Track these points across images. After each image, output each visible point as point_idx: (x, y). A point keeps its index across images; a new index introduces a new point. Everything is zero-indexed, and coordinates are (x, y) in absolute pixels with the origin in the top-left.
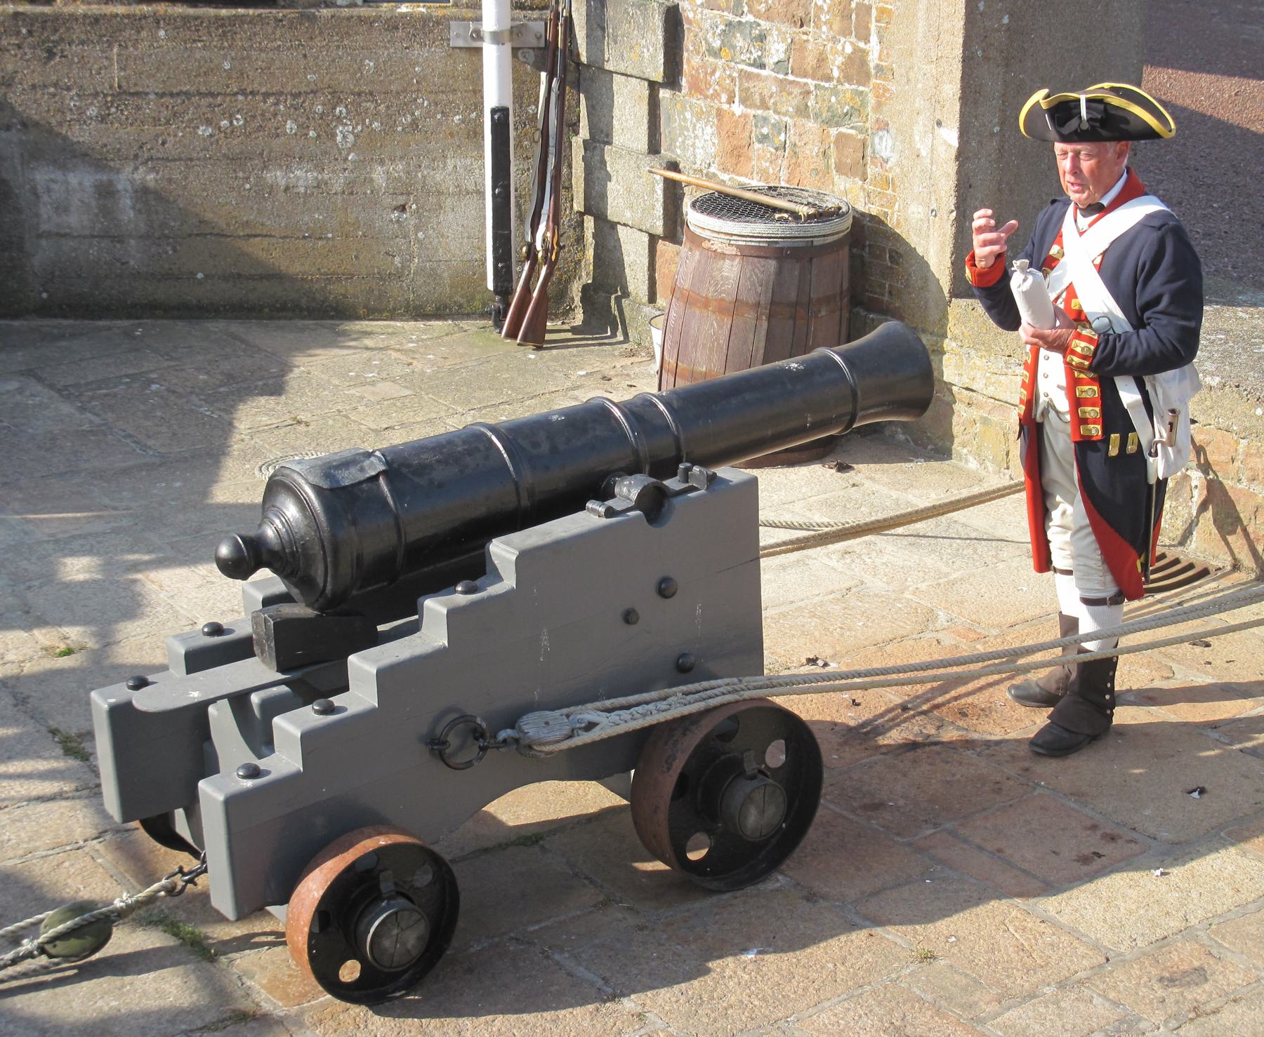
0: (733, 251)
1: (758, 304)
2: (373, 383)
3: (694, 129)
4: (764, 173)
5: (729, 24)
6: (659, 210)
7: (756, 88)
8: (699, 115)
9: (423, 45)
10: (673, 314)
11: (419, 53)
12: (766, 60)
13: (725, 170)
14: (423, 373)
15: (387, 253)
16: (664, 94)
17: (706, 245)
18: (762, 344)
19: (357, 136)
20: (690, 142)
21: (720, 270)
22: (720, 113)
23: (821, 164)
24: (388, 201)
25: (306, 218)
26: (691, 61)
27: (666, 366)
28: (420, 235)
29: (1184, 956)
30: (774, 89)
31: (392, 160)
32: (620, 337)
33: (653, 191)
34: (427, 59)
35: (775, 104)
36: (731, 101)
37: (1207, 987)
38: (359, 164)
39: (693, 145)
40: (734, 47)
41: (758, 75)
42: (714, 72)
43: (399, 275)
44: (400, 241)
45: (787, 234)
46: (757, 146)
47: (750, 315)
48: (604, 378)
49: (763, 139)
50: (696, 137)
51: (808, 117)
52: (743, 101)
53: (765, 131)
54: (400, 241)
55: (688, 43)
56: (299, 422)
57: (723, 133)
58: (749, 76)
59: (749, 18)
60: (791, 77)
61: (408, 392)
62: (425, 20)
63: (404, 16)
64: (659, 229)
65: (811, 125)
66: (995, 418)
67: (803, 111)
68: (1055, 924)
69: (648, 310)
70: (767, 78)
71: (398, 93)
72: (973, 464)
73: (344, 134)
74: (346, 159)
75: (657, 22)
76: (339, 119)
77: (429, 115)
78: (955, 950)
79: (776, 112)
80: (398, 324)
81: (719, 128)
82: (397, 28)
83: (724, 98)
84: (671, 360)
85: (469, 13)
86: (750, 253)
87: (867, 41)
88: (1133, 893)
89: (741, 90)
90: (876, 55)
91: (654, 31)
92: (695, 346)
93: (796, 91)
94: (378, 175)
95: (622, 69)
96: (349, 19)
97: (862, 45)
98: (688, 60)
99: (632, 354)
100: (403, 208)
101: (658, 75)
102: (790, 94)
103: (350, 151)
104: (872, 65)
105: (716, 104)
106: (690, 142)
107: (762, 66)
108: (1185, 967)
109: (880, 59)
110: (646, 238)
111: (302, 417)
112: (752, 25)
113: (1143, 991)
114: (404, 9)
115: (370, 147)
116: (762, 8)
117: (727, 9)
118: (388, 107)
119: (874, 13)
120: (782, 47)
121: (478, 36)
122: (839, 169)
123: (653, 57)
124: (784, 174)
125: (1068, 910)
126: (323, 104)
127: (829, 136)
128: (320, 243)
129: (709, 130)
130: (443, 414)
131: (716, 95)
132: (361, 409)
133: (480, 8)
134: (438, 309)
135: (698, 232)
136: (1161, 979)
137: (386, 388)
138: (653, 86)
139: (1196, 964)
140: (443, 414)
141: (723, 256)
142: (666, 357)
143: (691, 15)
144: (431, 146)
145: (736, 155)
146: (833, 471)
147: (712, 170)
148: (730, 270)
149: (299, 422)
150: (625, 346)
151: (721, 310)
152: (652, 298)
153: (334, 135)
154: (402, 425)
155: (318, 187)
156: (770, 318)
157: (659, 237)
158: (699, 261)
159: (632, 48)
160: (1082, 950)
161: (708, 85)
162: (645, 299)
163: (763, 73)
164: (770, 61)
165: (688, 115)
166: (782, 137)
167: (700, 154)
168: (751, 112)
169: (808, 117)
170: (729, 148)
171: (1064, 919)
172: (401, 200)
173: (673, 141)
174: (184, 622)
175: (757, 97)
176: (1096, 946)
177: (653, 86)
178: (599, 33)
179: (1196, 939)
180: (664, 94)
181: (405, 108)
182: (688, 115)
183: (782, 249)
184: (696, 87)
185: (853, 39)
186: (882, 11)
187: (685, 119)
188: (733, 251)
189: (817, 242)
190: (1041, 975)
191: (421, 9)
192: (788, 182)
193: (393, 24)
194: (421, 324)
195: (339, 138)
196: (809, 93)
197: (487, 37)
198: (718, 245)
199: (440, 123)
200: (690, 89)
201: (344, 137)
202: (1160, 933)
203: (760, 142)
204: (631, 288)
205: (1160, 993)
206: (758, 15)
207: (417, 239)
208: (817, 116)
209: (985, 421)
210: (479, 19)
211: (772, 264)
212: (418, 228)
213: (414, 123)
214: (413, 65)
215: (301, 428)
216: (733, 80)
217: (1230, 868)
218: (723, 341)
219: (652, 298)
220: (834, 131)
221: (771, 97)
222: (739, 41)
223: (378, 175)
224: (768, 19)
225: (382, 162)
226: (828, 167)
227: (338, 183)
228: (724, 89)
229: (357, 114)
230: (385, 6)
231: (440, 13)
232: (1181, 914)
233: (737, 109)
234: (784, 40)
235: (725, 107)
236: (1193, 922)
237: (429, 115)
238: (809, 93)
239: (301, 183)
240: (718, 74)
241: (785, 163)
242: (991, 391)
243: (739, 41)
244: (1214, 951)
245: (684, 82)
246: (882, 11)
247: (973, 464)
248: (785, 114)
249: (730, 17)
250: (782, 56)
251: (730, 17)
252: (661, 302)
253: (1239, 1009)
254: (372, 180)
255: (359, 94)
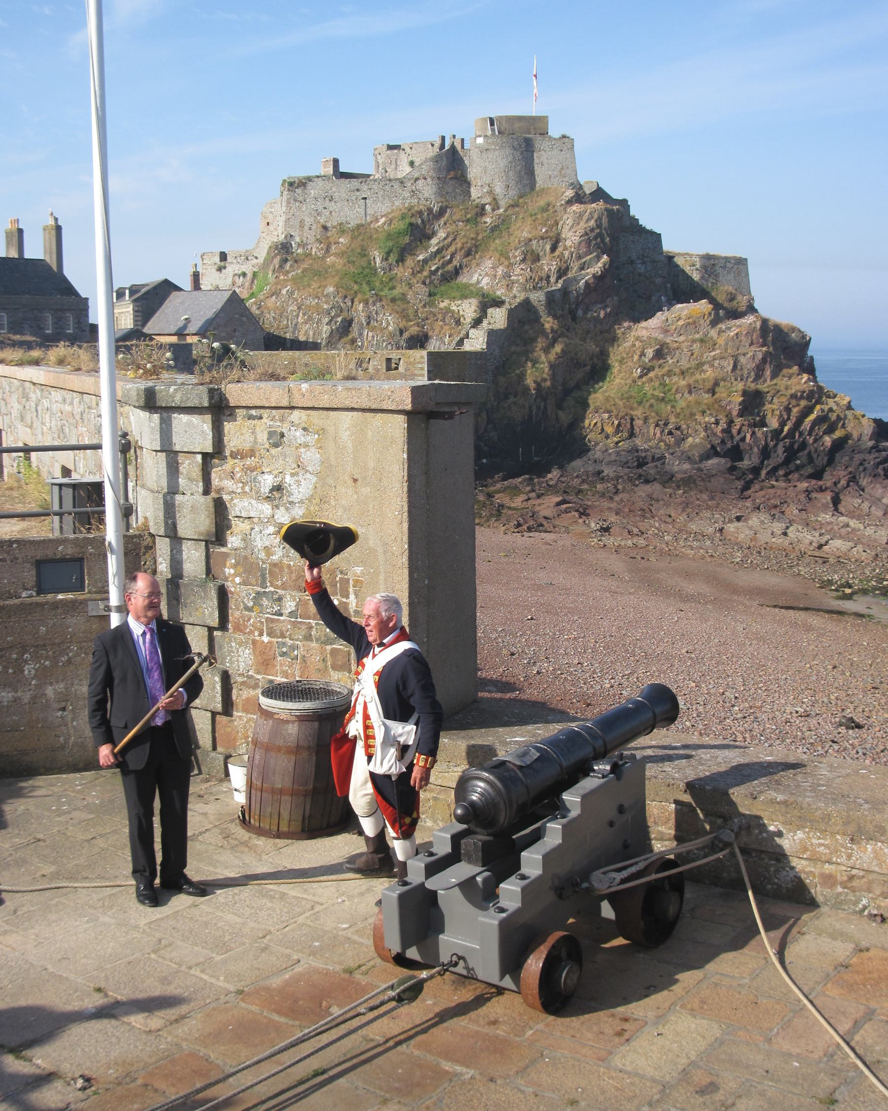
0: (294, 718)
1: (309, 748)
2: (69, 812)
3: (238, 652)
4: (285, 674)
5: (258, 593)
6: (219, 698)
7: (277, 627)
8: (240, 644)
9: (72, 616)
10: (257, 757)
11: (71, 621)
12: (283, 611)
13: (258, 673)
14: (94, 803)
15: (56, 736)
16: (216, 633)
17: (276, 716)
18: (313, 769)
19: (36, 670)
20: (235, 659)
21: (287, 730)
22: (254, 642)
23: (321, 665)
24: (56, 705)
25: (8, 719)
26: (234, 614)
27: (254, 786)
28: (75, 723)
29: (700, 1078)
30: (289, 627)
31: (57, 682)
32: (196, 772)
33: (214, 688)
34: (75, 624)
35: (290, 635)
36: (261, 634)
37: (721, 1091)
38: (38, 686)
39: (237, 661)
40: (262, 605)
41: (278, 620)
42: (249, 620)
43: (63, 747)
44: (63, 728)
45: (323, 706)
46: (279, 658)
47: (305, 754)
48: (199, 796)
49: (283, 654)
50: (239, 656)
51: (312, 640)
52: (269, 635)
53: (284, 650)
54: (63, 728)
55: (232, 605)
56: (39, 840)
57: (257, 653)
58: (272, 621)
59: (272, 589)
60: (299, 620)
61: (92, 816)
62: (73, 602)
63: (61, 600)
64: (219, 707)
65: (314, 644)
66: (441, 797)
67: (308, 638)
68: (627, 1072)
69: (213, 754)
70: (284, 621)
71: (59, 644)
72: (429, 823)
73: (29, 670)
74: (30, 684)
75: (213, 594)
76: (26, 662)
77: (77, 654)
78: (584, 1096)
79: (291, 639)
80: (64, 776)
81: (254, 650)
82: (58, 608)
83: (256, 633)
84: (257, 782)
85: (98, 596)
86: (303, 719)
87: (347, 597)
88: (654, 1048)
89: (267, 629)
90: (354, 605)
91: (211, 600)
92: (274, 774)
93: (303, 627)
94: (50, 691)
95: (191, 620)
96: (31, 604)
97: (344, 600)
98: (232, 615)
99: (207, 780)
100: (64, 709)
101: (215, 622)
102: (300, 629)
103: (33, 679)
104: (351, 611)
105: (252, 637)
106: (235, 659)
107: (281, 615)
108: (704, 1083)
109: (357, 606)
110: (209, 715)
111: (41, 836)
112: (272, 593)
113: (692, 1100)
114: (60, 597)
115: (44, 676)
116: (279, 583)
117: (257, 585)
118: (54, 653)
119: (351, 582)
120: (293, 604)
121: (108, 609)
122: (335, 667)
123: (211, 614)
124: (297, 673)
125: (627, 1063)
126: (17, 654)
127: (326, 650)
128: (17, 733)
129: (247, 651)
130: (120, 826)
131: (251, 632)
132: (71, 828)
133: (108, 593)
134: (86, 765)
135: (270, 709)
136: (697, 1092)
137: (77, 814)
138: (211, 629)
139: (709, 1080)
140: (120, 826)
141: (288, 722)
142: (254, 781)
143: (233, 589)
144: (79, 673)
145: (265, 663)
146: (355, 836)
147: (250, 673)
148: (293, 730)
149: (39, 840)
150: (201, 776)
151: (289, 751)
152: (214, 748)
153: (23, 671)
154: (101, 836)
155: (15, 701)
156: (317, 753)
157: (219, 713)
158: (272, 726)
159: (197, 609)
160: (648, 1084)
161: (246, 627)
162: (210, 749)
163: (281, 618)
164: (286, 612)
165: (233, 644)
166: (296, 653)
167: (242, 665)
168: (275, 640)
169: (312, 640)
170: (261, 661)
171: (629, 1068)
172: (63, 704)
173: (224, 659)
174: (40, 969)
175: (278, 631)
176: (654, 1080)
177: (211, 629)
178: (175, 602)
179: (699, 1067)
180: (216, 633)
181: (63, 652)
182: (233, 644)
183: (320, 716)
184: (237, 628)
185: (339, 597)
186: (356, 582)
187: (231, 647)
188: (294, 718)
189: (338, 709)
190: (636, 1102)
191: (70, 596)
192: (301, 677)
193: (56, 605)
194: (78, 775)
195: (26, 672)
196: (312, 627)
197: (113, 610)
198: (283, 716)
199: (83, 659)
200: (234, 630)
201: (30, 671)
202: (680, 1067)
203: (281, 656)
204: (201, 743)
205: (701, 1100)
206: (276, 587)
207: (73, 727)
208: (317, 640)
209: (435, 799)
210: (108, 599)
211: (316, 725)
212: (73, 720)
213: (69, 661)
214: (68, 628)
215: (41, 843)
216: (262, 623)
217: (693, 1026)
218: (291, 769)
219: (214, 748)
220: (329, 648)
221: (287, 631)
222: (265, 602)
223: (50, 691)
224: (283, 589)
225: (51, 684)
226: (326, 667)
227: (26, 697)
228: (256, 629)
229: (36, 658)
230: (50, 596)
231: (82, 597)
232: (684, 1055)
233: (266, 639)
234: (294, 600)
235: (258, 638)
236: (693, 1058)
237: (77, 654)
238: (312, 627)
239: (5, 699)
240: (252, 621)
241: (298, 667)
242: (439, 782)
243: (265, 602)
244: (713, 1072)
245: (230, 626)
246: (356, 582)
247: (429, 823)
248: (297, 640)
249: (259, 589)
250: (293, 609)
251: (259, 589)
252: (219, 749)
253: (744, 1100)
254: (46, 694)
255: (37, 646)
